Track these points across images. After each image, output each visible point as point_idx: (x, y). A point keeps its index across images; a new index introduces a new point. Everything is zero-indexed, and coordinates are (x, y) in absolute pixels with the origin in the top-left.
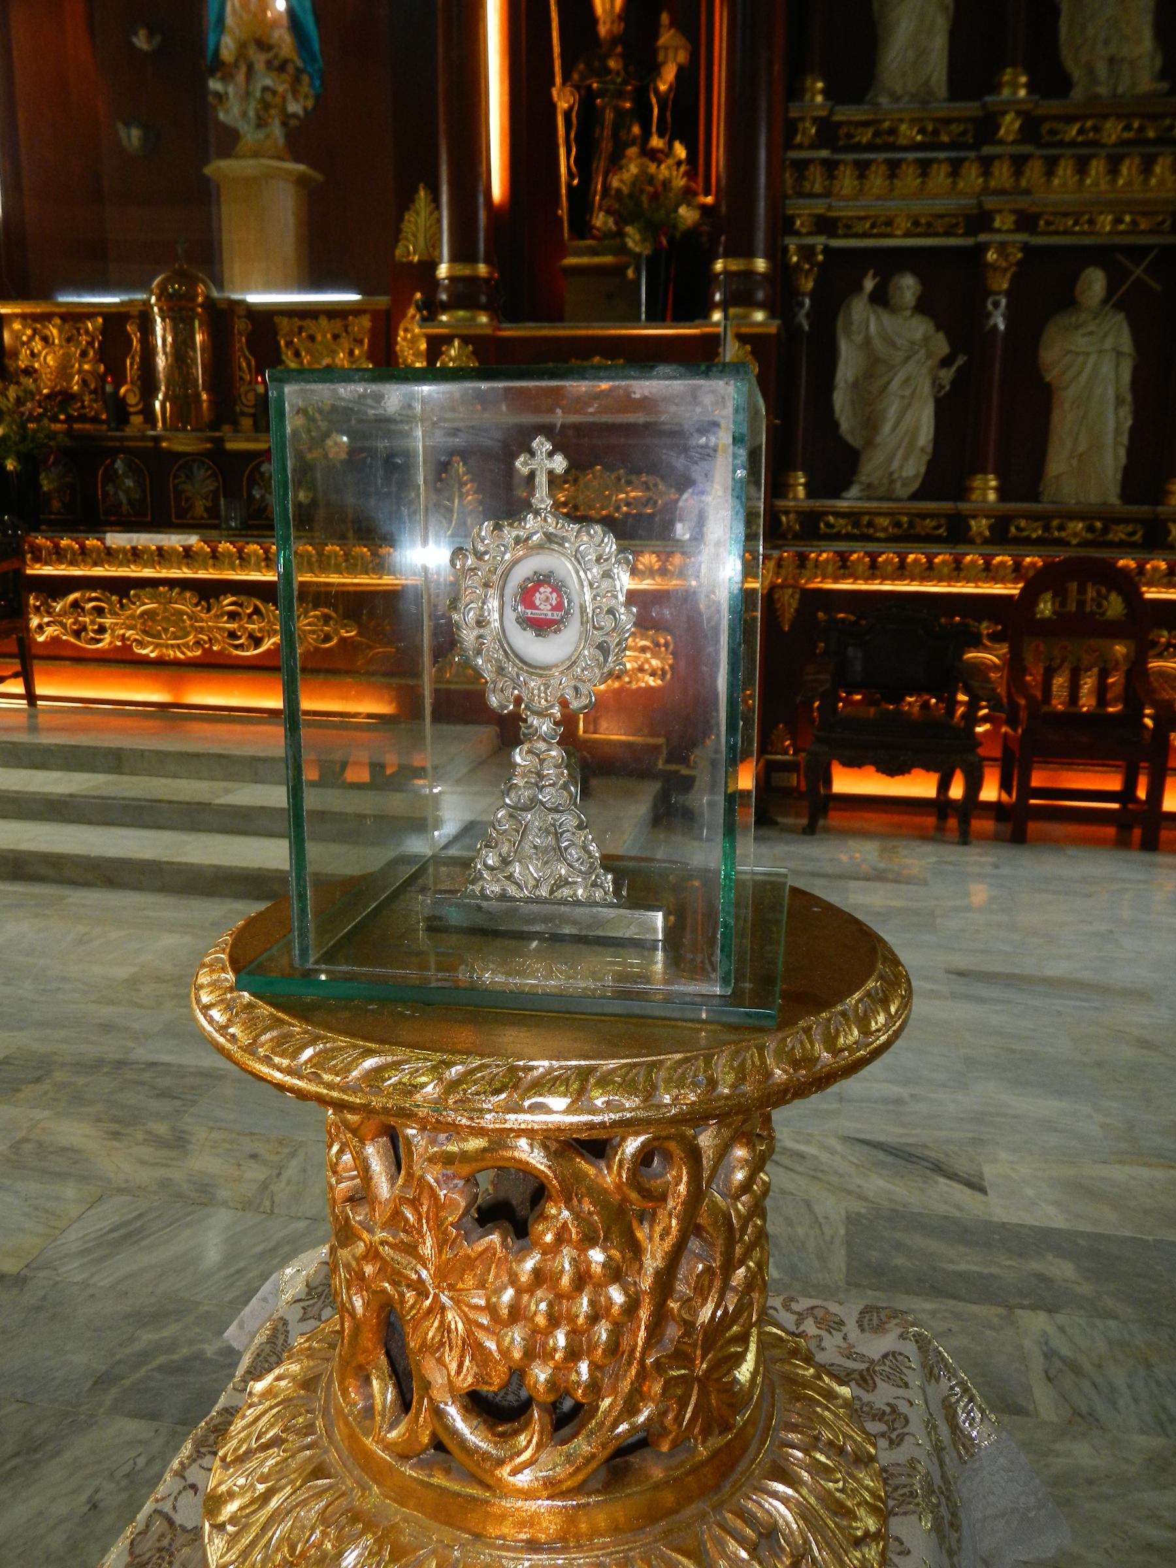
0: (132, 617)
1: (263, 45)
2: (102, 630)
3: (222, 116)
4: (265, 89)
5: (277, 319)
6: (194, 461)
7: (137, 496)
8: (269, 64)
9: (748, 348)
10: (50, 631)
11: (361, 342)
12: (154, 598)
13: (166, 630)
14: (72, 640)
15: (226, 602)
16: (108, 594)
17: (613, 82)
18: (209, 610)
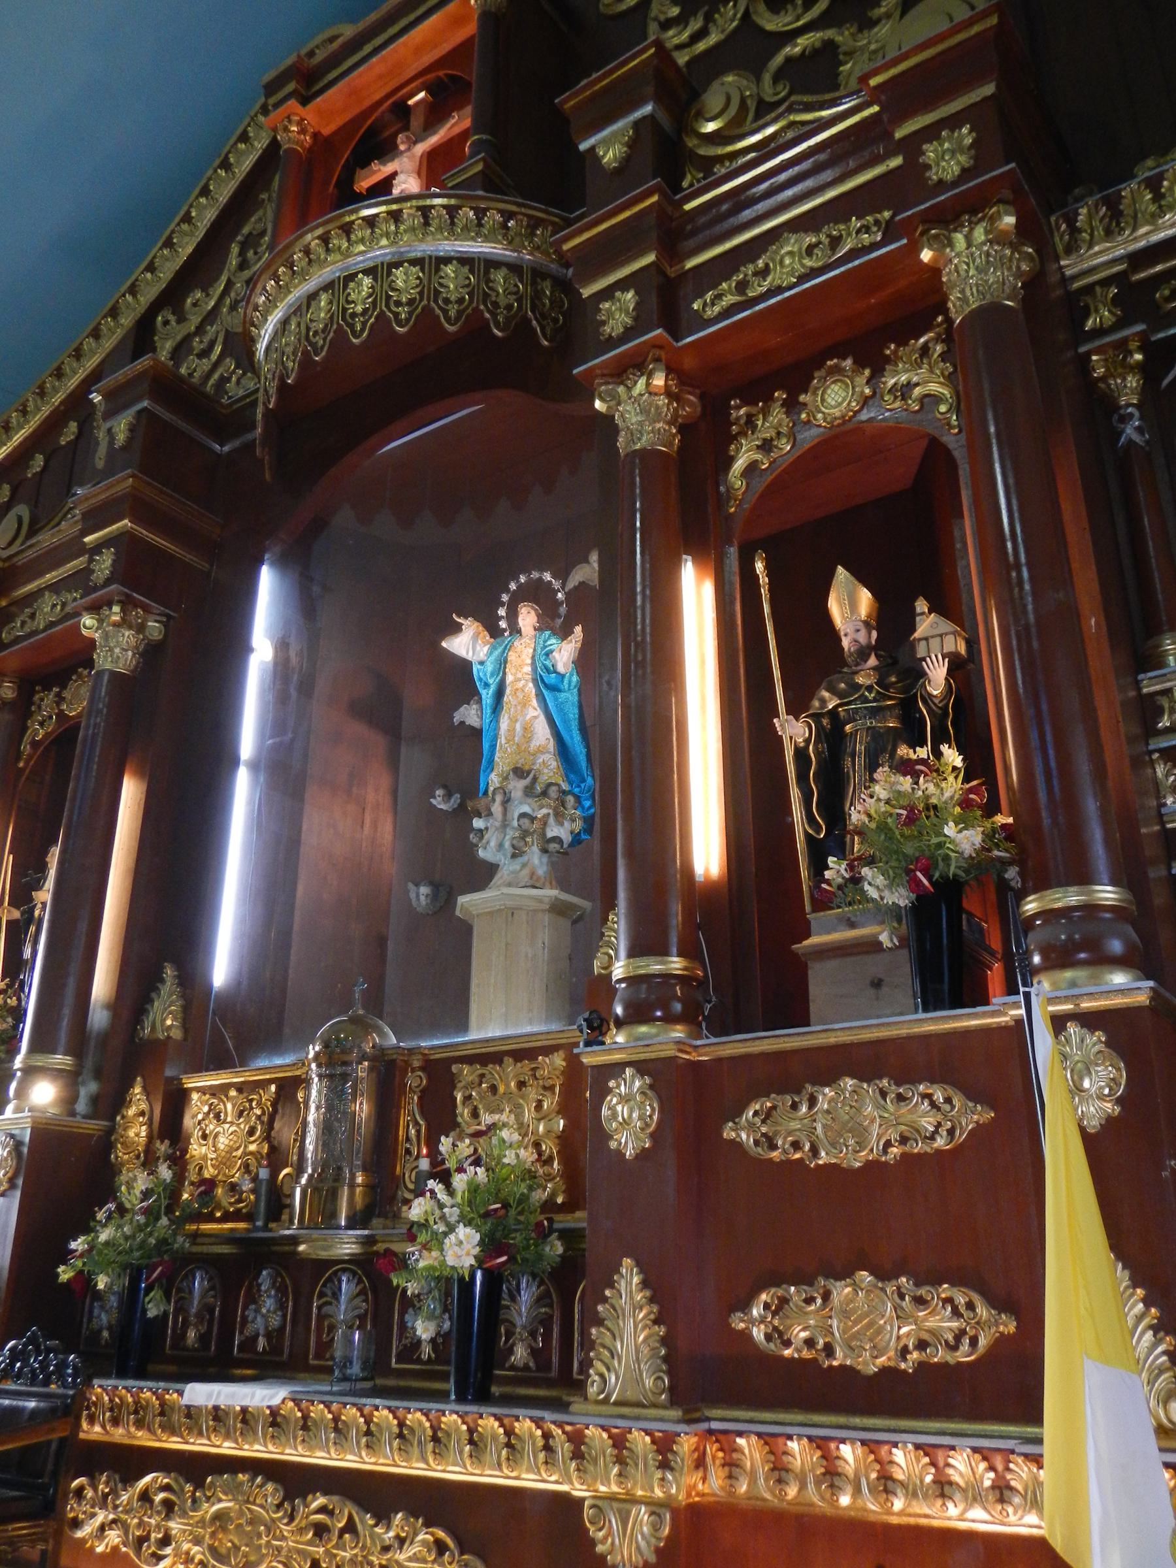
0: (202, 1522)
1: (519, 772)
2: (166, 1541)
3: (481, 853)
4: (523, 815)
5: (455, 1068)
6: (344, 1270)
7: (275, 1321)
8: (529, 791)
9: (1100, 1035)
10: (114, 1537)
11: (551, 1088)
12: (233, 1490)
13: (237, 1548)
14: (132, 1555)
15: (315, 1505)
16: (181, 1480)
17: (867, 701)
18: (292, 1518)
